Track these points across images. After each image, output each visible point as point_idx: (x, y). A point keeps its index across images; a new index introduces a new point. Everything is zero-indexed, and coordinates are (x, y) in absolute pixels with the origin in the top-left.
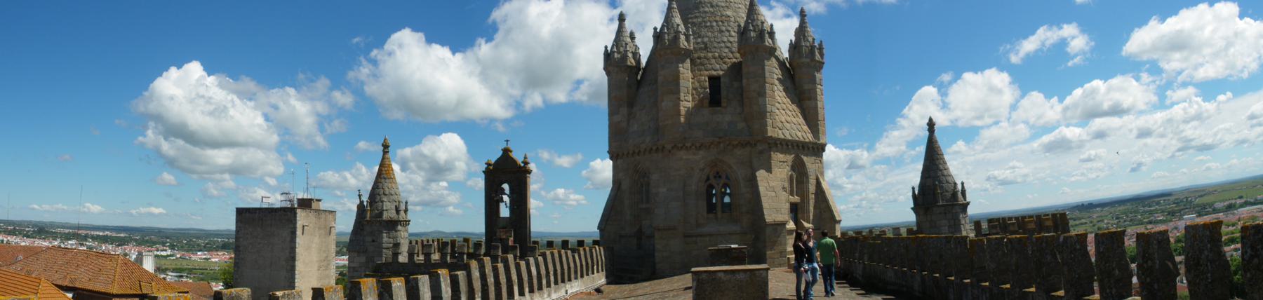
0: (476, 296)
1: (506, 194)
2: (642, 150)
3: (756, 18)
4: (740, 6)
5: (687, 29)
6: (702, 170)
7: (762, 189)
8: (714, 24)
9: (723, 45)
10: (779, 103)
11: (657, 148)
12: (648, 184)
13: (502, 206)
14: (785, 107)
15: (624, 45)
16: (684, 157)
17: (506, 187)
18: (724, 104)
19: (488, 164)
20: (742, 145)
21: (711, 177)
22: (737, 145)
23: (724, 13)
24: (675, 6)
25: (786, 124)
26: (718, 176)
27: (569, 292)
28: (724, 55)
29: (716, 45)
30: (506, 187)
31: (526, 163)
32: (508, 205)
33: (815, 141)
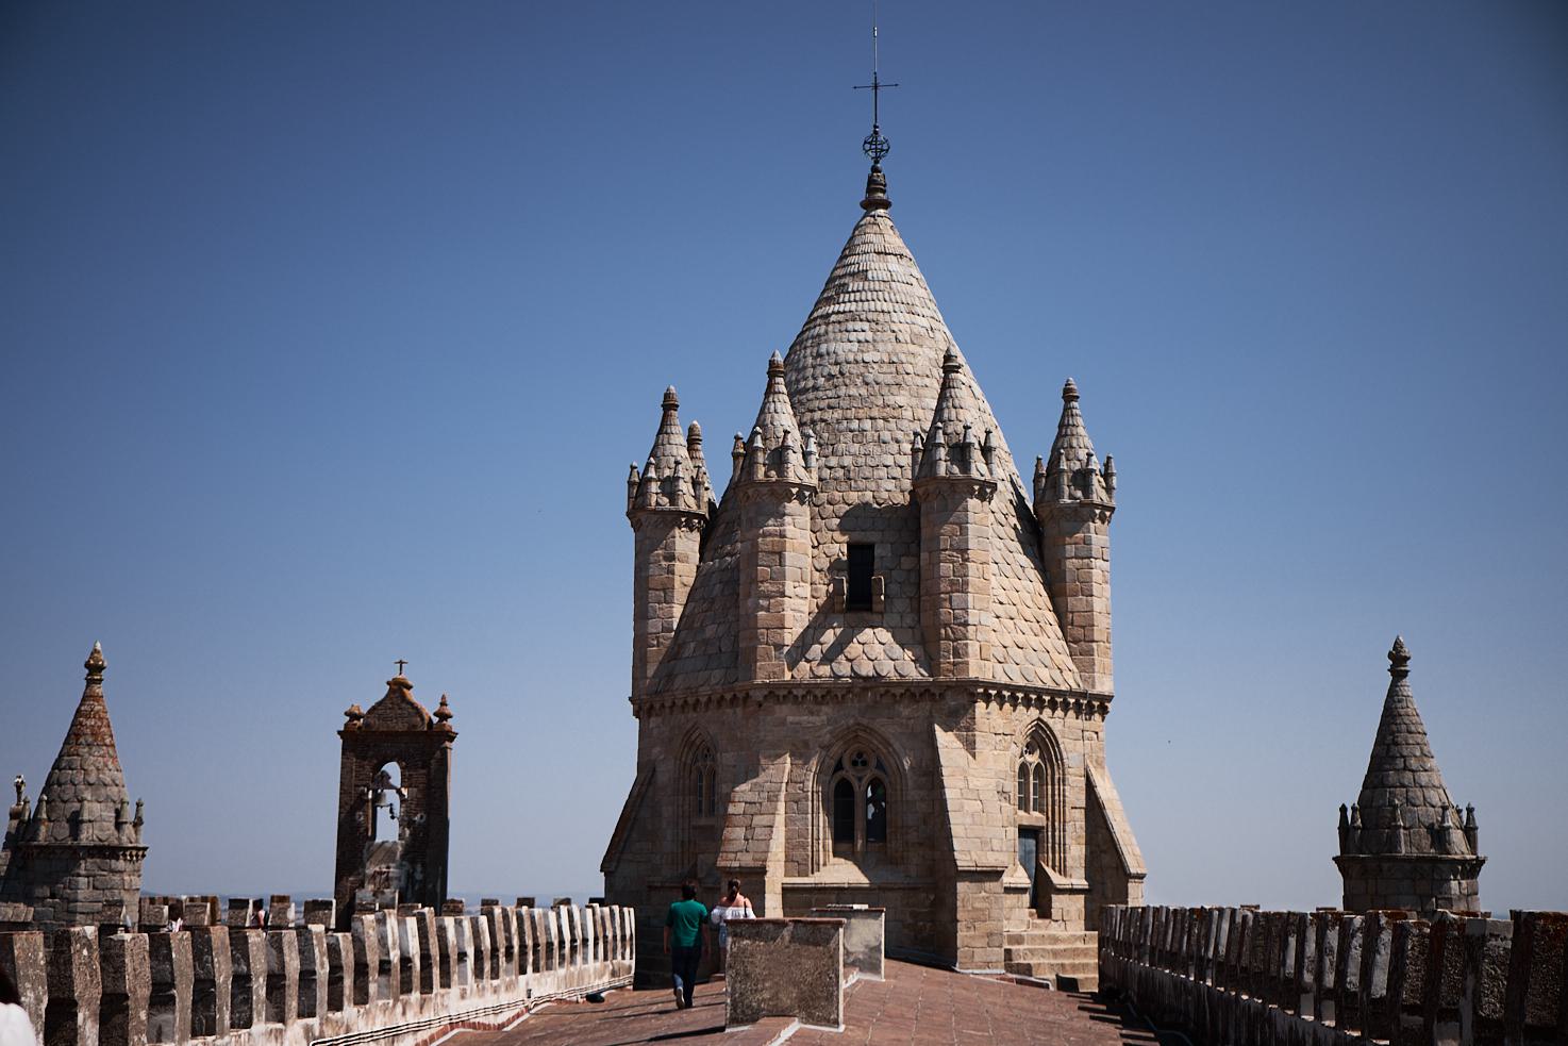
0: (371, 978)
1: (392, 787)
2: (703, 700)
3: (953, 417)
5: (806, 437)
6: (826, 747)
7: (951, 794)
8: (867, 424)
10: (1001, 603)
11: (735, 695)
12: (713, 774)
13: (383, 814)
15: (673, 465)
16: (790, 719)
17: (393, 769)
19: (353, 716)
20: (913, 695)
21: (846, 763)
22: (902, 695)
23: (891, 400)
24: (783, 388)
26: (860, 761)
27: (535, 994)
30: (393, 769)
31: (443, 716)
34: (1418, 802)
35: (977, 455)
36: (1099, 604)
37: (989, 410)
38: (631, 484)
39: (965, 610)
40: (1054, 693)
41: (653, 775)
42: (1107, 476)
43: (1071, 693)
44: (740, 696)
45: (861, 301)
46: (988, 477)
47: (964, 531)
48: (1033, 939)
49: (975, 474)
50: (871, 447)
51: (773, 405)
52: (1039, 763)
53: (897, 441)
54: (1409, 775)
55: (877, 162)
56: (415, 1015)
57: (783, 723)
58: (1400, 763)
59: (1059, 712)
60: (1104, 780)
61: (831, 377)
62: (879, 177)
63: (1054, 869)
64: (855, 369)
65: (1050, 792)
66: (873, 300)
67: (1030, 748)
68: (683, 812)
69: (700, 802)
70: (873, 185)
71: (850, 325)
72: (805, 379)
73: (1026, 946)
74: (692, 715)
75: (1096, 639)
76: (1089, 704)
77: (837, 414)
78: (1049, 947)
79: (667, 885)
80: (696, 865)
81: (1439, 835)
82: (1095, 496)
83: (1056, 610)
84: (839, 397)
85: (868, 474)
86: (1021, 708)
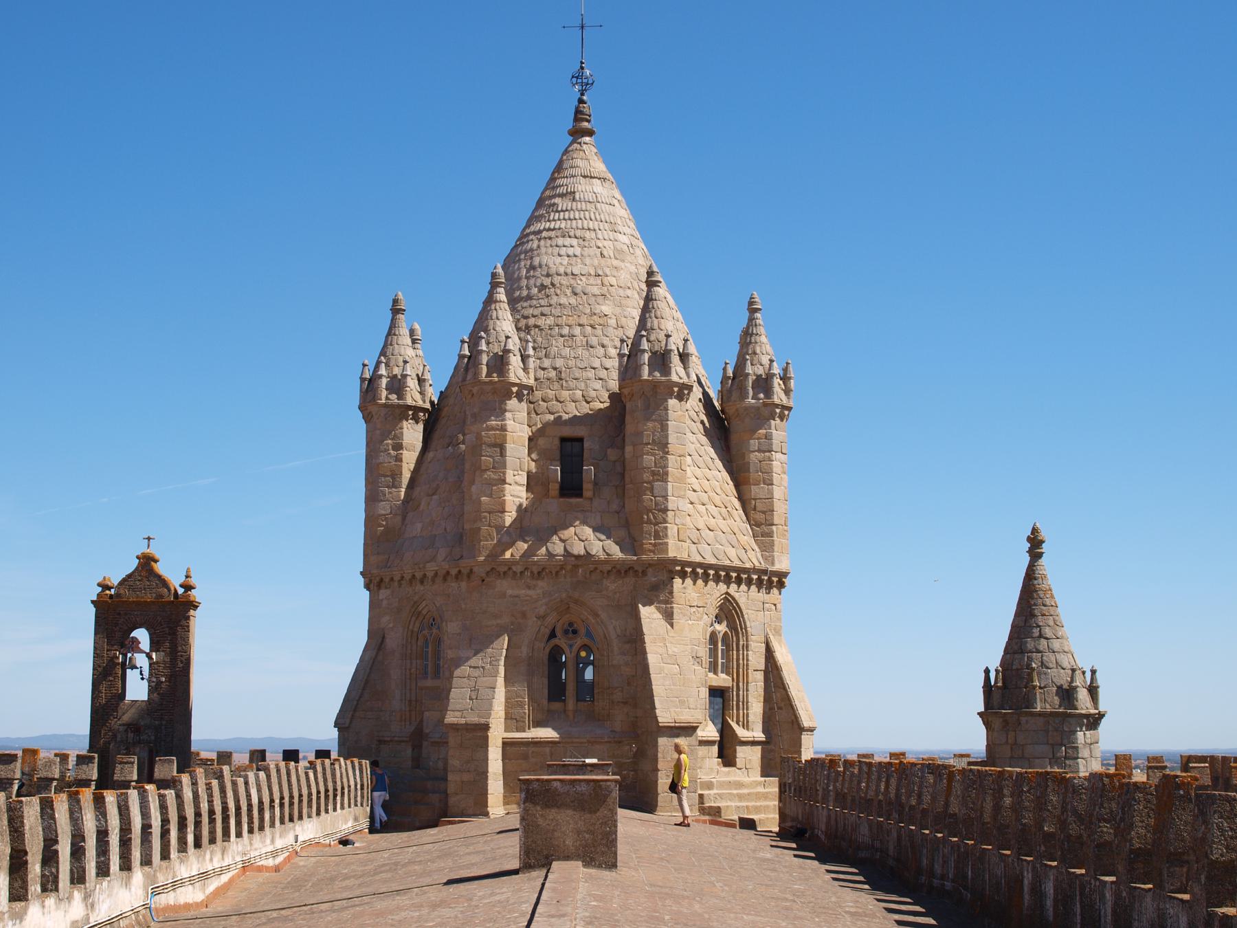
1: (142, 652)
2: (430, 575)
3: (656, 327)
4: (629, 292)
6: (542, 618)
7: (652, 659)
8: (577, 331)
9: (591, 374)
10: (694, 491)
11: (460, 572)
12: (439, 641)
13: (131, 675)
14: (706, 500)
15: (401, 364)
16: (510, 592)
17: (142, 636)
18: (588, 492)
19: (105, 587)
21: (559, 632)
22: (609, 572)
25: (706, 533)
26: (571, 631)
27: (301, 839)
28: (593, 394)
29: (577, 374)
30: (142, 636)
31: (188, 587)
32: (146, 673)
33: (764, 566)
34: (1051, 666)
35: (675, 359)
36: (778, 492)
37: (681, 318)
38: (362, 380)
39: (665, 497)
40: (740, 570)
41: (382, 641)
42: (785, 378)
43: (755, 570)
44: (465, 571)
45: (570, 219)
46: (685, 380)
47: (664, 428)
48: (722, 785)
49: (674, 378)
50: (580, 351)
51: (495, 313)
52: (726, 632)
53: (603, 346)
54: (1043, 642)
55: (582, 94)
56: (219, 861)
57: (503, 595)
58: (1036, 632)
59: (744, 587)
60: (781, 647)
61: (542, 287)
62: (585, 108)
63: (738, 723)
64: (565, 281)
65: (735, 657)
66: (580, 219)
67: (718, 619)
68: (411, 674)
69: (426, 666)
70: (579, 115)
71: (560, 241)
72: (520, 288)
73: (715, 791)
74: (419, 587)
75: (775, 523)
76: (770, 581)
77: (550, 321)
78: (735, 792)
79: (396, 739)
80: (422, 721)
81: (1067, 694)
82: (775, 396)
83: (740, 498)
84: (551, 305)
85: (577, 375)
86: (711, 583)
